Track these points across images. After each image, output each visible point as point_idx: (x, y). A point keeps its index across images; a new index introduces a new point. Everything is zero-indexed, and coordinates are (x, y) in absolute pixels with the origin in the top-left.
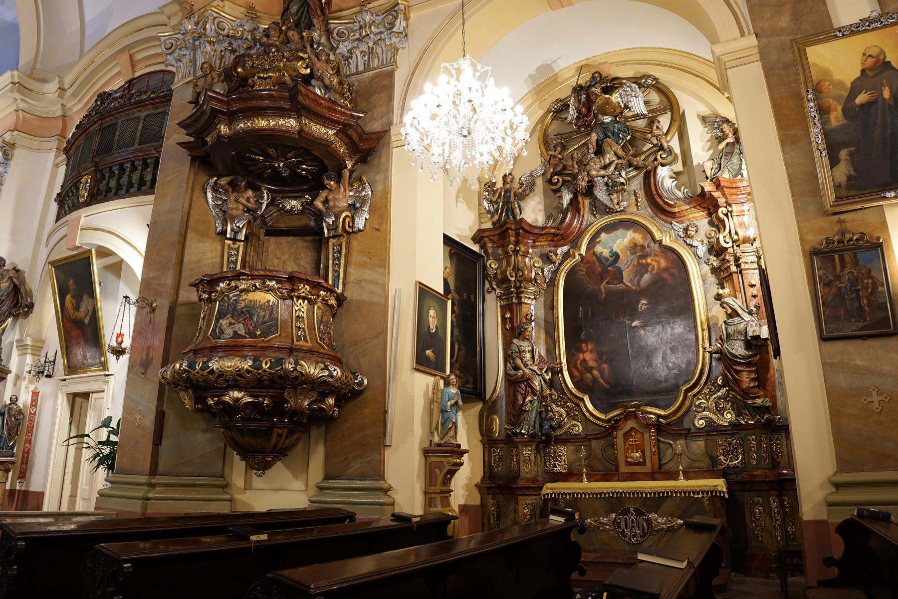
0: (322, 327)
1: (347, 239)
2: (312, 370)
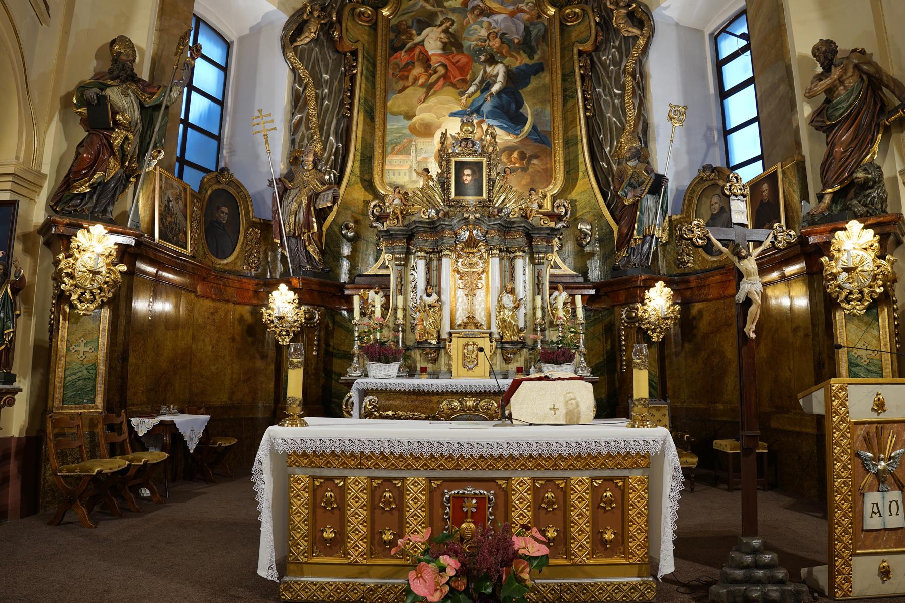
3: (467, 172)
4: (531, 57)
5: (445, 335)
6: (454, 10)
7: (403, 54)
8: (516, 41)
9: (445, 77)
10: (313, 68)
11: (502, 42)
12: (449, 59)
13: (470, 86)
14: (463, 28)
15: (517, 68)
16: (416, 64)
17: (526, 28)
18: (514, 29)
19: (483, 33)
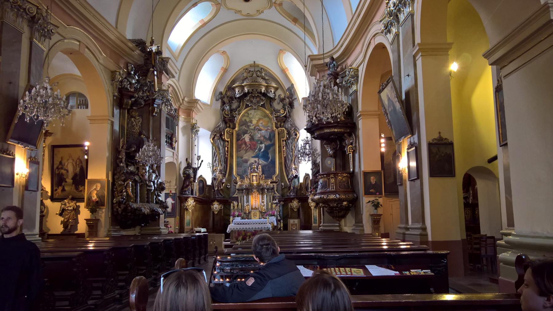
0: (340, 184)
1: (352, 153)
2: (332, 197)
3: (254, 177)
4: (271, 142)
5: (250, 211)
6: (252, 129)
7: (240, 141)
8: (267, 138)
9: (250, 147)
10: (218, 145)
11: (264, 138)
12: (251, 143)
13: (256, 150)
14: (254, 134)
15: (268, 145)
16: (243, 144)
17: (270, 134)
18: (267, 134)
19: (259, 136)
